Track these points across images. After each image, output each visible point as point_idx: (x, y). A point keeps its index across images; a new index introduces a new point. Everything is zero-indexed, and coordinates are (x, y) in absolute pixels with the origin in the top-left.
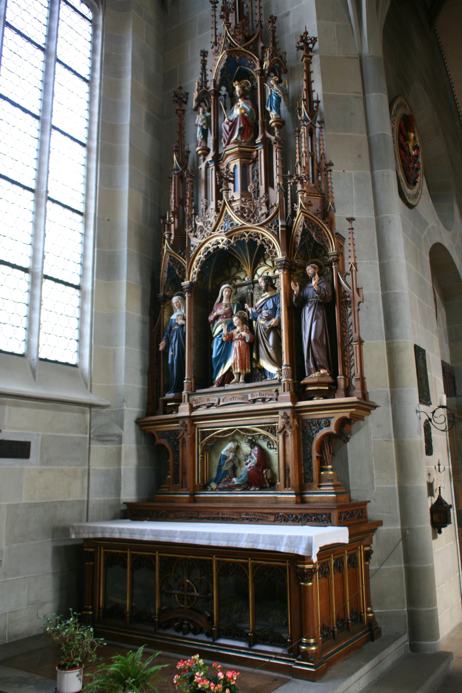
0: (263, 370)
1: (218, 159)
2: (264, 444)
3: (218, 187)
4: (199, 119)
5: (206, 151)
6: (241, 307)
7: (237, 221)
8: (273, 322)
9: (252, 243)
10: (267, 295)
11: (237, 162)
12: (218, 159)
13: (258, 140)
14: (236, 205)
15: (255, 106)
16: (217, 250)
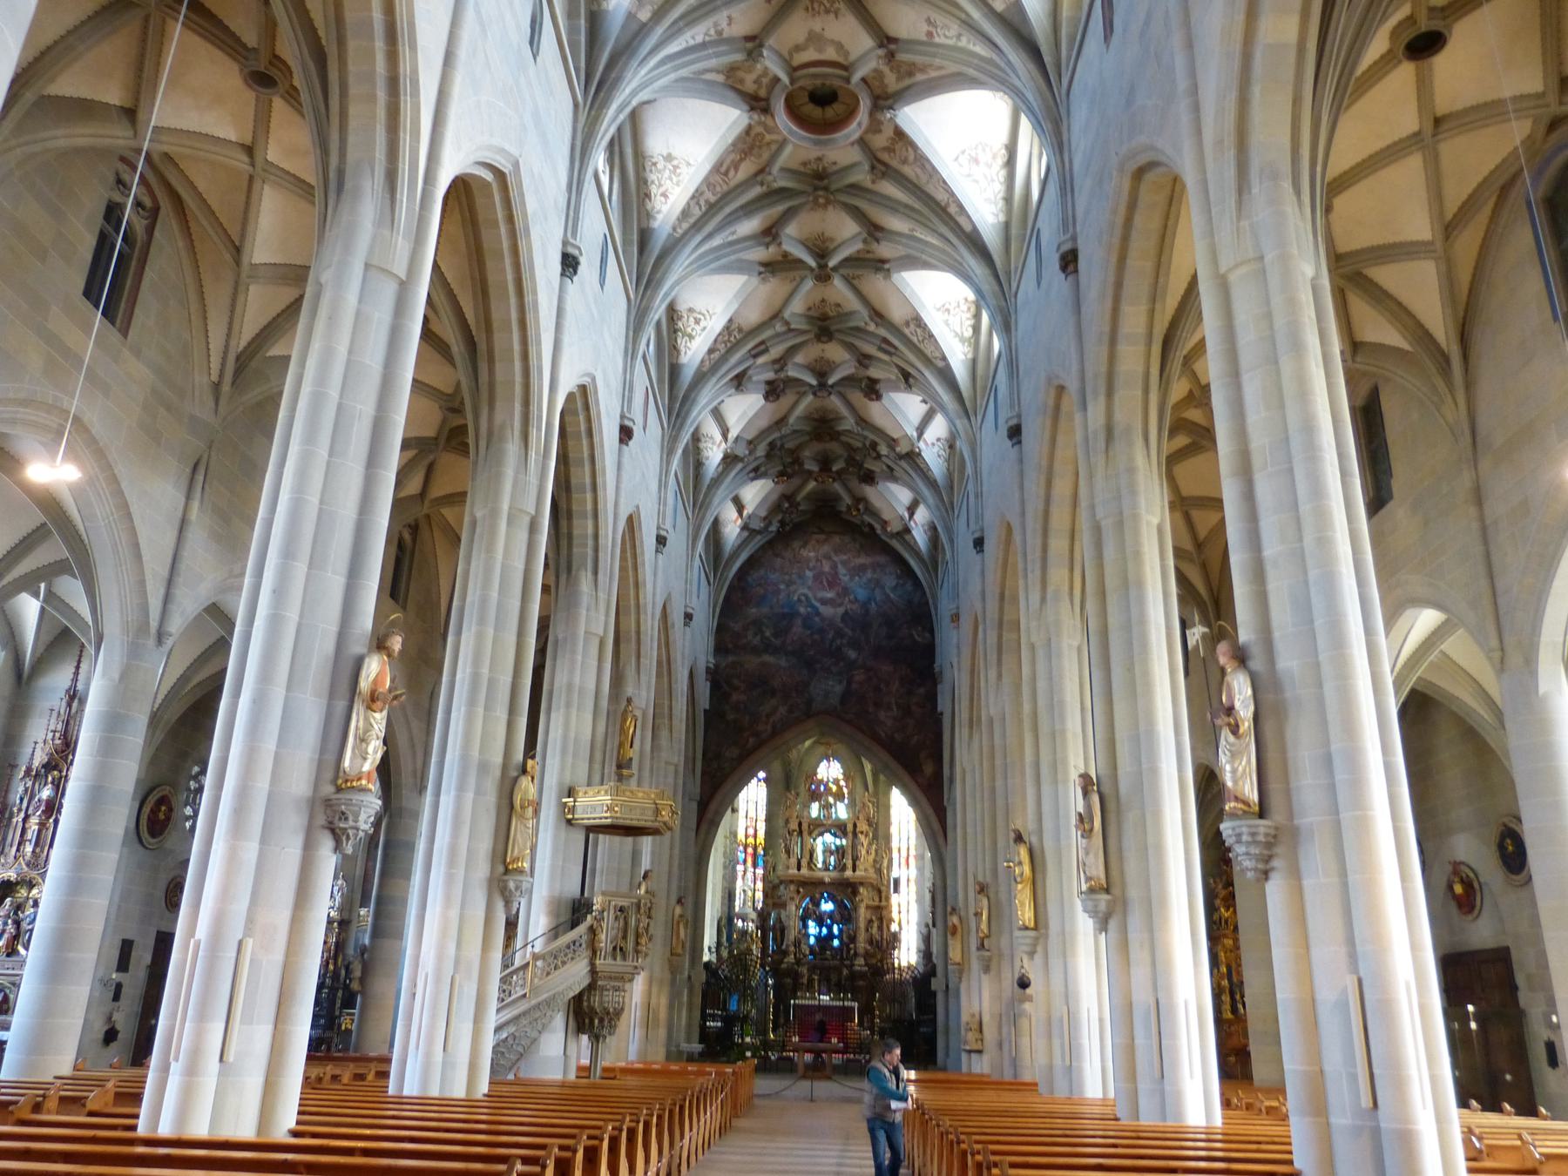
0: (18, 952)
1: (25, 820)
2: (8, 991)
3: (20, 844)
4: (21, 789)
5: (20, 810)
6: (16, 913)
7: (24, 867)
8: (30, 927)
9: (30, 882)
10: (32, 910)
11: (37, 827)
12: (25, 820)
13: (51, 820)
14: (27, 858)
15: (57, 794)
16: (8, 880)
